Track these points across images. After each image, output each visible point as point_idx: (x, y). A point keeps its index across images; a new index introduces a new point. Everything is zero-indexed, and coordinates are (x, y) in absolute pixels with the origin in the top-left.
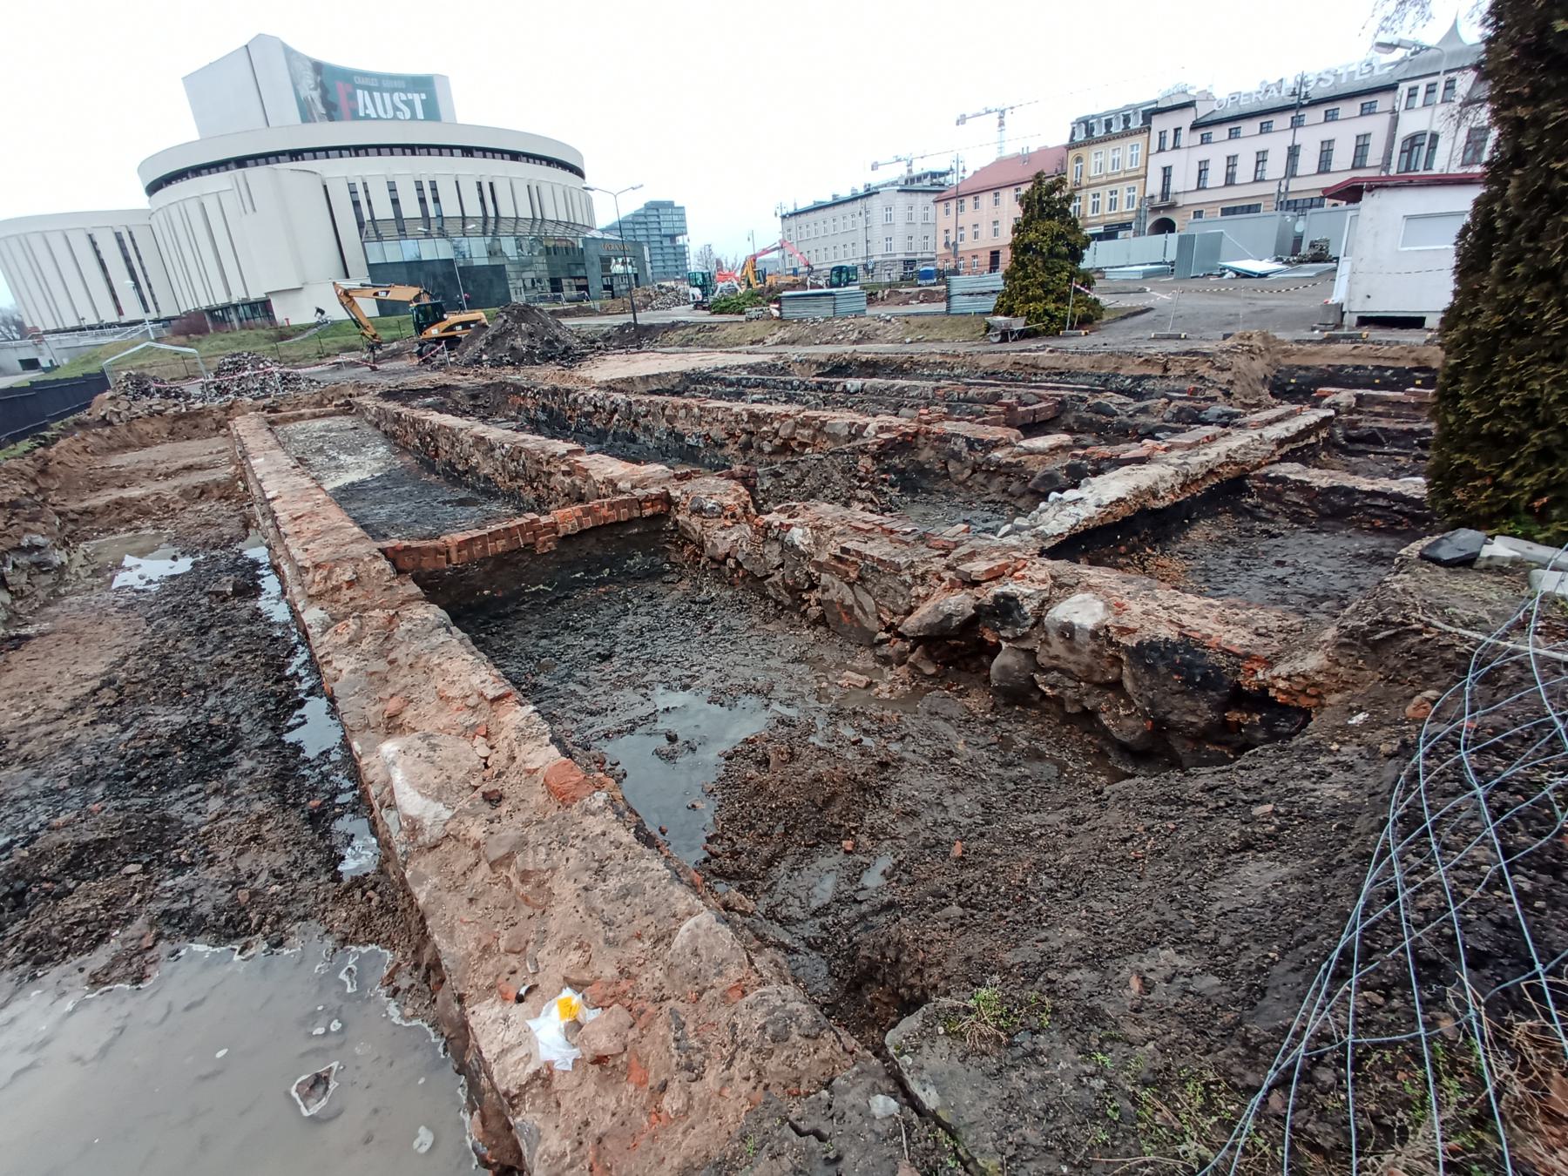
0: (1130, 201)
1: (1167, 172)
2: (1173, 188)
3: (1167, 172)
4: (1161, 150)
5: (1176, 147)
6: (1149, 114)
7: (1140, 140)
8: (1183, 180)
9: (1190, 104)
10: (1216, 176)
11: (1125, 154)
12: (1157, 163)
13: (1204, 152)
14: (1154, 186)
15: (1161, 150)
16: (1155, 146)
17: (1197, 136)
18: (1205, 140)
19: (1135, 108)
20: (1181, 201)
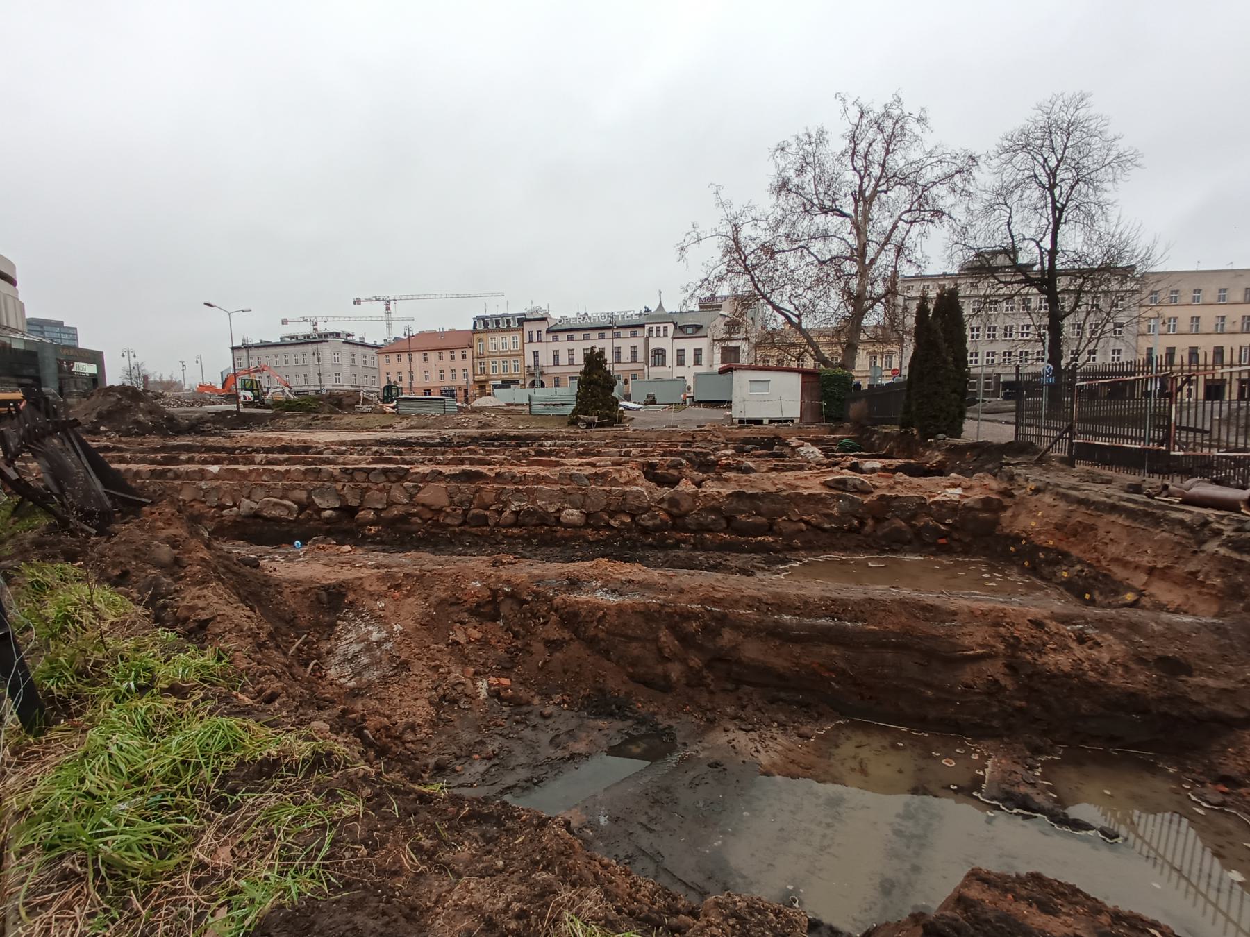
0: (516, 368)
1: (536, 354)
3: (536, 354)
4: (531, 341)
5: (539, 341)
6: (522, 321)
7: (518, 334)
8: (546, 359)
9: (544, 319)
10: (563, 359)
11: (508, 341)
12: (529, 349)
13: (555, 346)
14: (530, 361)
16: (527, 339)
17: (550, 337)
18: (556, 339)
19: (513, 316)
20: (546, 371)
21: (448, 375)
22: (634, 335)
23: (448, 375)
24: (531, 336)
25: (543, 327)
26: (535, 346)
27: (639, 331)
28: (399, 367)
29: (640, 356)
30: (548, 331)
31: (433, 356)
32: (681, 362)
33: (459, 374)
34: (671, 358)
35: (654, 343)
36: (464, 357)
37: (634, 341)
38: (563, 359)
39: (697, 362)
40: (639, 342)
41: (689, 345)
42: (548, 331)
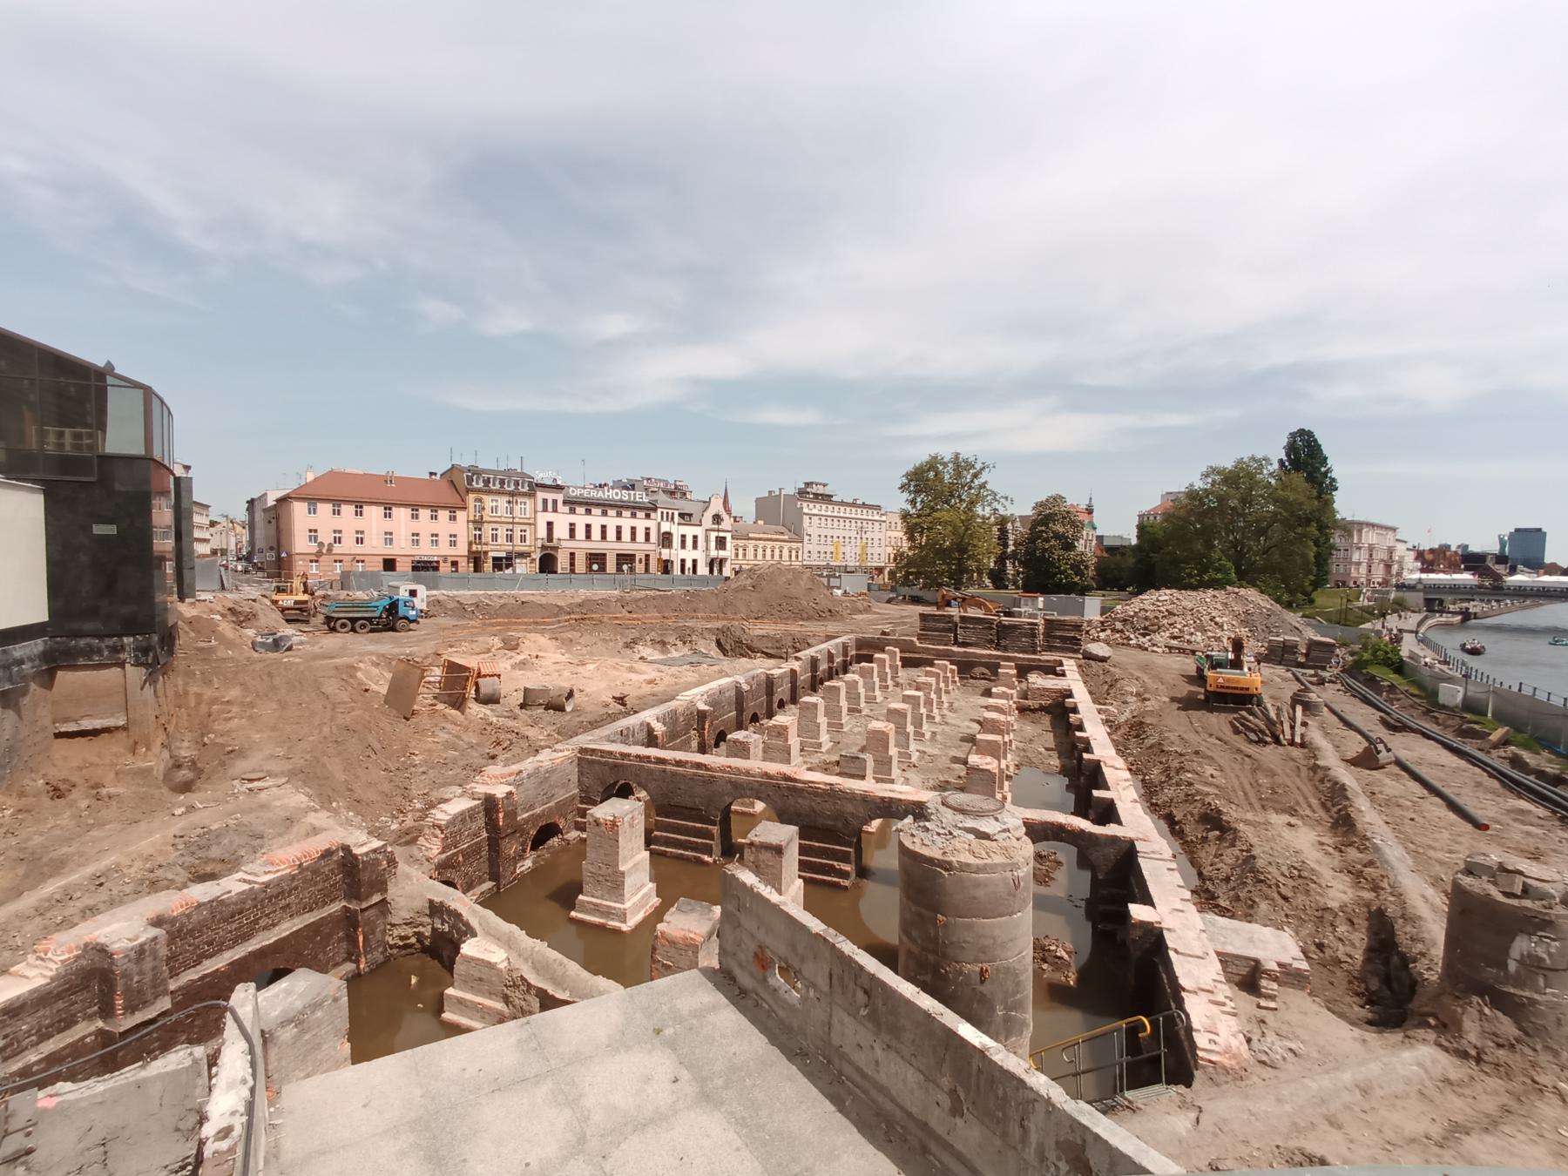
1: (550, 524)
2: (556, 536)
3: (550, 524)
4: (545, 510)
5: (555, 510)
8: (561, 532)
14: (542, 532)
15: (545, 510)
16: (540, 506)
20: (564, 544)
21: (425, 540)
22: (648, 516)
23: (425, 540)
24: (545, 501)
25: (560, 497)
26: (550, 516)
27: (653, 515)
28: (337, 522)
29: (653, 537)
30: (565, 503)
31: (402, 514)
32: (683, 546)
33: (444, 540)
34: (676, 541)
35: (665, 527)
36: (453, 518)
37: (648, 523)
38: (580, 533)
39: (695, 546)
40: (652, 524)
41: (690, 531)
42: (565, 503)
